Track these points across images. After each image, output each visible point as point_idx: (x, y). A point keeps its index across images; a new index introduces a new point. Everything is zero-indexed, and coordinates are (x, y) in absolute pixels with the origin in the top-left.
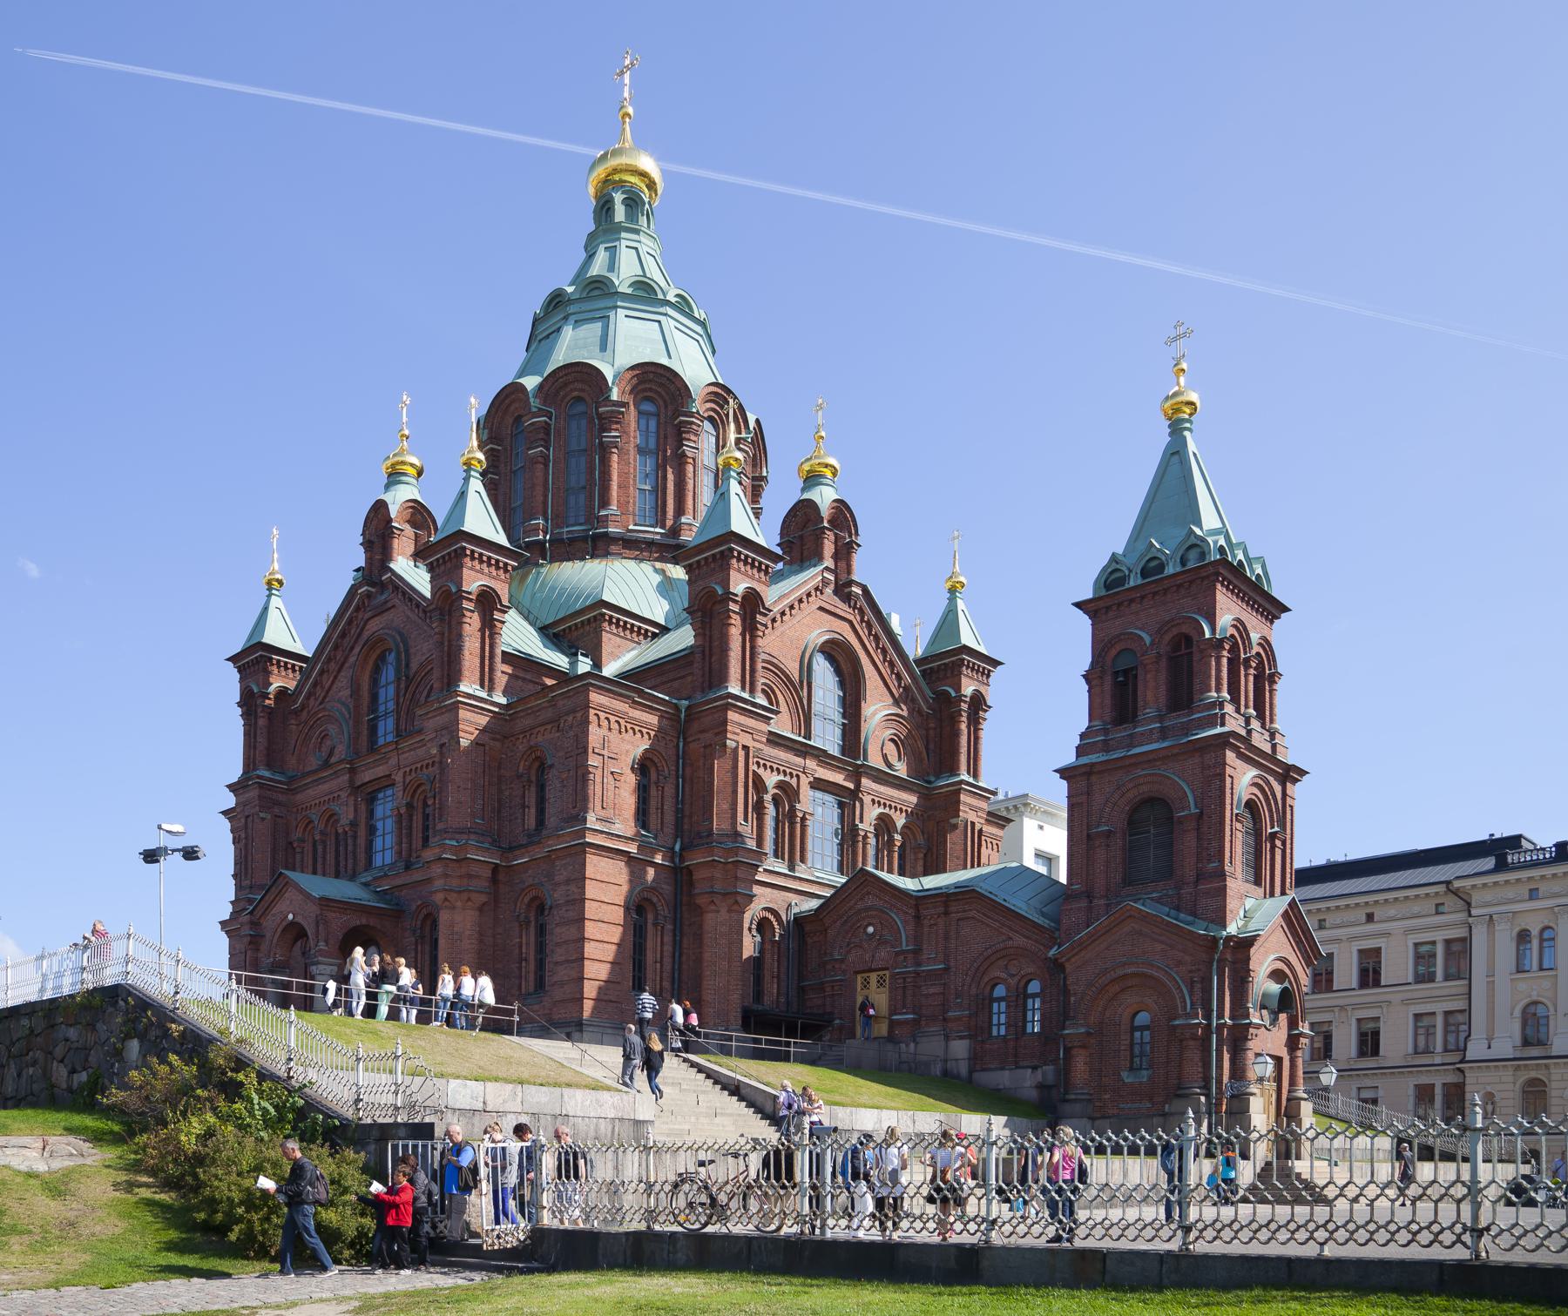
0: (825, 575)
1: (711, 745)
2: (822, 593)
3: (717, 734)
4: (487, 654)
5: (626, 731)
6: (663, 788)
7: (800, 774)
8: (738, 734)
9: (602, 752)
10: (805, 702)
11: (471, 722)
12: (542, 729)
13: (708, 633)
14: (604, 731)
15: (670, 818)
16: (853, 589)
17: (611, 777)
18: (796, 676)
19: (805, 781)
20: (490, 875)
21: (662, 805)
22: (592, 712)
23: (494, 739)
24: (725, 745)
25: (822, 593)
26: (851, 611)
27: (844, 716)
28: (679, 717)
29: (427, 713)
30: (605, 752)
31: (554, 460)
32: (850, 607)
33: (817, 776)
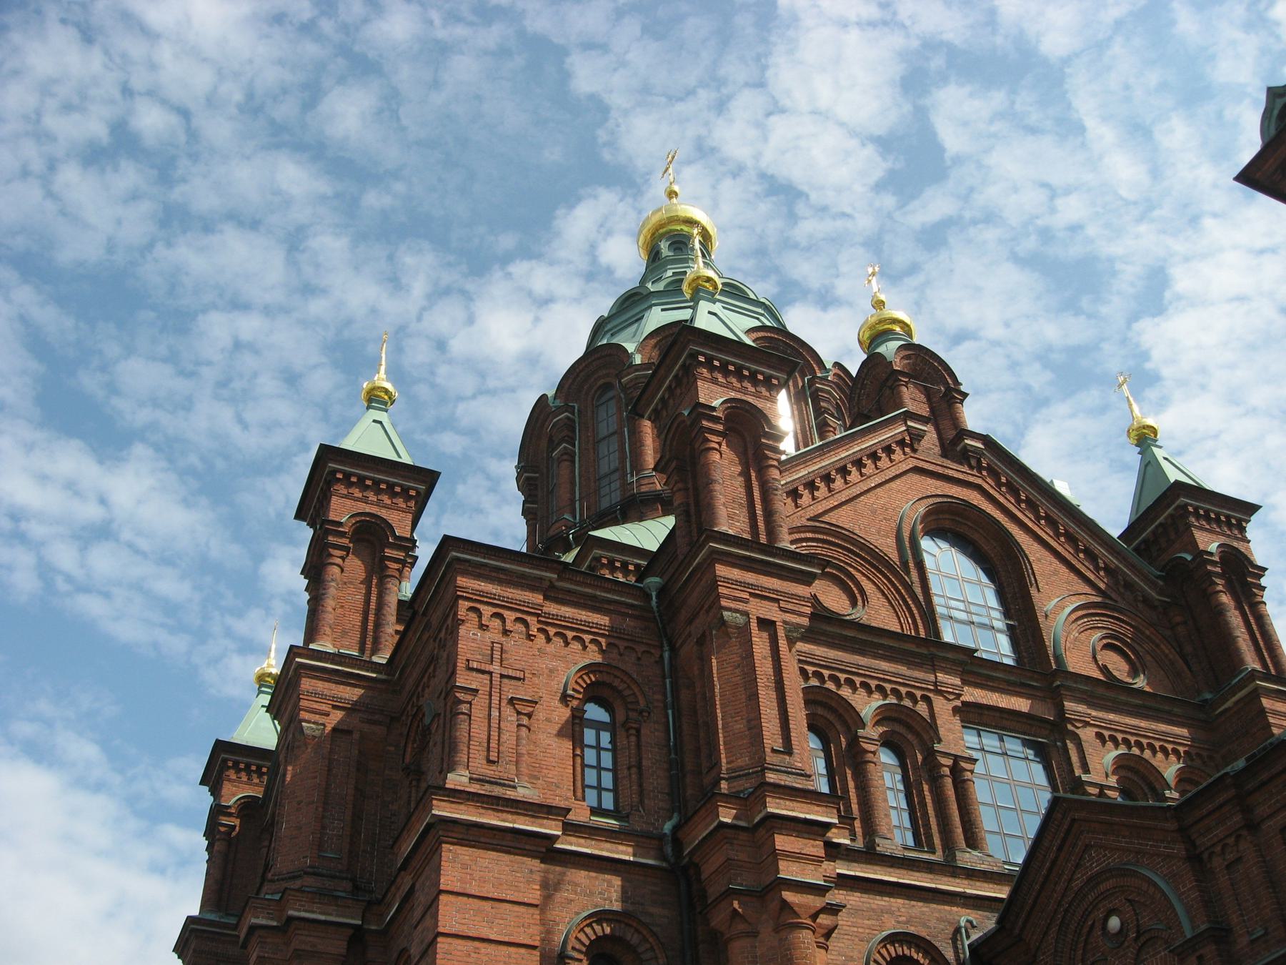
0: (910, 423)
1: (703, 635)
2: (914, 451)
3: (708, 612)
4: (373, 606)
5: (549, 640)
6: (638, 731)
7: (931, 695)
8: (746, 601)
9: (488, 667)
10: (918, 590)
13: (690, 485)
14: (494, 635)
16: (966, 441)
17: (508, 711)
18: (894, 556)
20: (343, 951)
22: (463, 605)
24: (723, 622)
25: (914, 451)
26: (975, 472)
27: (1007, 614)
28: (650, 610)
30: (495, 668)
32: (971, 468)
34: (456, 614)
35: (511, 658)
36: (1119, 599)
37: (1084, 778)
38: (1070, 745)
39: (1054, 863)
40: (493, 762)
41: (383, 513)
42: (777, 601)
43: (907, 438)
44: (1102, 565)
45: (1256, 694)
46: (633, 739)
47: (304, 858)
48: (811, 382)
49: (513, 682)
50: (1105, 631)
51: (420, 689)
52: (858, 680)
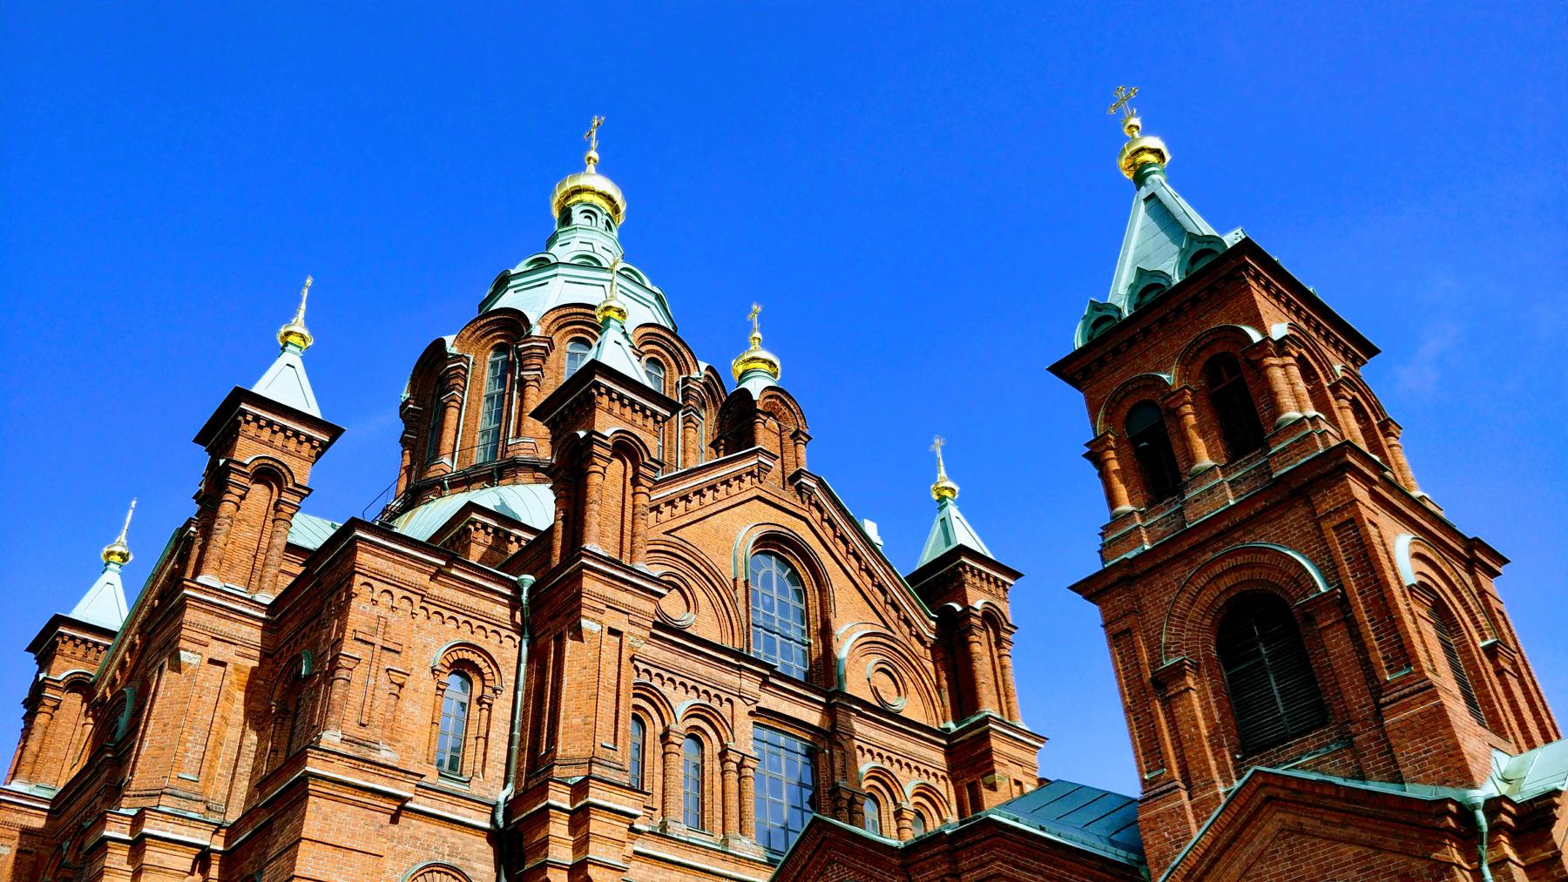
7: (735, 699)
8: (602, 612)
11: (205, 628)
12: (306, 630)
15: (498, 751)
16: (802, 480)
17: (383, 676)
19: (742, 708)
21: (487, 734)
22: (359, 579)
23: (244, 656)
25: (761, 482)
26: (805, 507)
29: (154, 629)
30: (378, 641)
31: (469, 403)
33: (762, 704)
34: (350, 587)
35: (392, 631)
36: (897, 631)
37: (842, 784)
38: (837, 752)
39: (804, 867)
40: (364, 725)
41: (285, 459)
42: (628, 614)
43: (756, 470)
44: (889, 601)
45: (985, 737)
46: (485, 713)
47: (163, 777)
48: (685, 381)
49: (391, 654)
50: (881, 657)
51: (299, 637)
52: (678, 679)
